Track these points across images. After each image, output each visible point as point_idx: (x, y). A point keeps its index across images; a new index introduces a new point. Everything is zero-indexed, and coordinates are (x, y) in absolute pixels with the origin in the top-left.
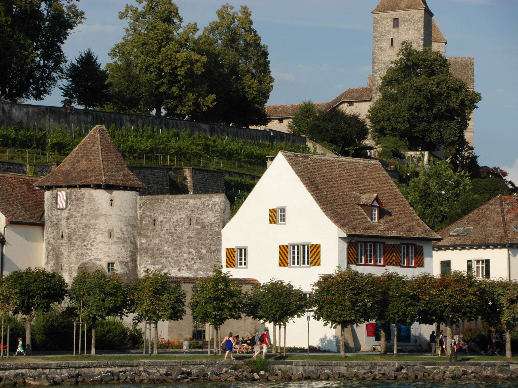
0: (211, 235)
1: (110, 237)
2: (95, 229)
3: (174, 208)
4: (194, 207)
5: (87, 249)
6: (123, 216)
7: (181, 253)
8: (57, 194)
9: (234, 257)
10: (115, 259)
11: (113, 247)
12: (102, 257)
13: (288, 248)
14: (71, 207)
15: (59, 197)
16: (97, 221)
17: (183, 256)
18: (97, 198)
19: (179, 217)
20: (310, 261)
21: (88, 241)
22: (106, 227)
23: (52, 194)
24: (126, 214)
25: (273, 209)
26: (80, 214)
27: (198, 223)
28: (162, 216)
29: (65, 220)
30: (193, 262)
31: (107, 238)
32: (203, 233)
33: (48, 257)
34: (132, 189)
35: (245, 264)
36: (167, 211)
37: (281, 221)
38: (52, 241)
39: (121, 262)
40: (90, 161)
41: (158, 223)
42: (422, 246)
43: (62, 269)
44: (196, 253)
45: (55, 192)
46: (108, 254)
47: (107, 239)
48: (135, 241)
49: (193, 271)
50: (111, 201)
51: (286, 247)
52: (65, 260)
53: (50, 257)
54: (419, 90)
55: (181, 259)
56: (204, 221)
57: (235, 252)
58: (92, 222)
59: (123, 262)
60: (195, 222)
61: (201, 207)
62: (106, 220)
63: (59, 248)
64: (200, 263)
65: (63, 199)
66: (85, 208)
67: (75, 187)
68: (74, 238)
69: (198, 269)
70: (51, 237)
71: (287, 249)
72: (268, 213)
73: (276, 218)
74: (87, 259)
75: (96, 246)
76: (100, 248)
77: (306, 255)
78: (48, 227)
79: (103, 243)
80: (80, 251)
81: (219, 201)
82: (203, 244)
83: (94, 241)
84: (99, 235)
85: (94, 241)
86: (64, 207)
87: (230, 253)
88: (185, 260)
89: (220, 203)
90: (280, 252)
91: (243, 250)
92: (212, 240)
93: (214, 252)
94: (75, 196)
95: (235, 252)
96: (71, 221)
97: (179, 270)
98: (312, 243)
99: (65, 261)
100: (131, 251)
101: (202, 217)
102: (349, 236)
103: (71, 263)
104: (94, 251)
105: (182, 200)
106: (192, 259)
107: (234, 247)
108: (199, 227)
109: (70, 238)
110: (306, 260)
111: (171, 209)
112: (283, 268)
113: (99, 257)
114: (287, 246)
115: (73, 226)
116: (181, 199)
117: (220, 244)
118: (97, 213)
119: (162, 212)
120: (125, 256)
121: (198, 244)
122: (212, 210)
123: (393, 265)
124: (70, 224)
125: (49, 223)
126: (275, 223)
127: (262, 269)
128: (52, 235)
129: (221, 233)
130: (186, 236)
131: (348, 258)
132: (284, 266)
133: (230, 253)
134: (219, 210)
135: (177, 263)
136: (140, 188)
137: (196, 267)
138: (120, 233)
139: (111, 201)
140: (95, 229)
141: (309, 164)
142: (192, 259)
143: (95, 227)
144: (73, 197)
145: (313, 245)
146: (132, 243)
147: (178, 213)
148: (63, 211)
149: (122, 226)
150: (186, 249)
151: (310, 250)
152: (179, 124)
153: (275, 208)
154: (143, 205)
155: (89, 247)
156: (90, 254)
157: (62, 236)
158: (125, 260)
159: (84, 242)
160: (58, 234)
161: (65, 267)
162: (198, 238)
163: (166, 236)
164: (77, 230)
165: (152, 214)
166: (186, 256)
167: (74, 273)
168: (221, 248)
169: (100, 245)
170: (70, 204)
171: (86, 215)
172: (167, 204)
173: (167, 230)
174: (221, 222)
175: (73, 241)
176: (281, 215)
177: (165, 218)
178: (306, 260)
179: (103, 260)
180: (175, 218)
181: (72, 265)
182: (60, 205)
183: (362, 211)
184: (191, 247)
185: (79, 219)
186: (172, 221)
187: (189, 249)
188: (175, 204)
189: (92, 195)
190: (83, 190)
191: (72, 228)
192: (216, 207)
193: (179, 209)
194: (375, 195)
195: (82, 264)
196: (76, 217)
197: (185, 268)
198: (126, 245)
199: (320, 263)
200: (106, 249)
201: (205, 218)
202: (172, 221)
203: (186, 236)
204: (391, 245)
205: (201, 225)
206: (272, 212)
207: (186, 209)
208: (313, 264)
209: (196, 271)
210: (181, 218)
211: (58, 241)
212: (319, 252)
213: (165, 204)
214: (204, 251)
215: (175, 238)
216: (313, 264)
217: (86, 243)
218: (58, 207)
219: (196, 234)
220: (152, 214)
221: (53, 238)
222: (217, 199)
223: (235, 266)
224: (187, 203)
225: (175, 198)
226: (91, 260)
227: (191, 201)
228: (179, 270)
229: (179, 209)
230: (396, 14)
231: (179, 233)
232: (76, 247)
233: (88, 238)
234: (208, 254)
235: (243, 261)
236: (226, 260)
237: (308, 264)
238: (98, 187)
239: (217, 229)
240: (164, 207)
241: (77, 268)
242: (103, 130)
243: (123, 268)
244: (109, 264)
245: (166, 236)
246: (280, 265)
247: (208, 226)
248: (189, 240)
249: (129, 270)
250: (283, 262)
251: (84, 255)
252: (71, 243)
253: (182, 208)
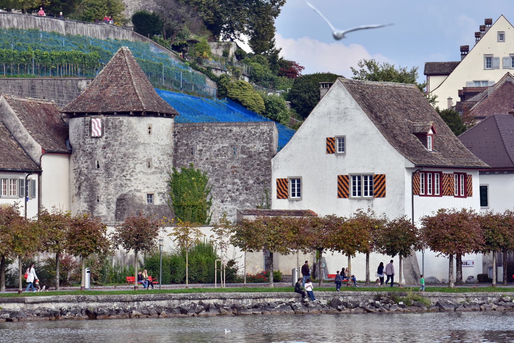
0: (258, 165)
1: (149, 167)
2: (134, 158)
3: (215, 136)
4: (238, 135)
5: (126, 180)
6: (160, 144)
7: (224, 183)
8: (91, 122)
9: (287, 188)
10: (153, 190)
11: (152, 177)
12: (142, 188)
13: (348, 179)
14: (108, 136)
15: (93, 125)
16: (136, 150)
17: (226, 187)
18: (135, 126)
19: (221, 145)
20: (374, 192)
21: (127, 171)
22: (144, 157)
23: (84, 122)
24: (163, 143)
25: (331, 138)
26: (118, 143)
27: (243, 152)
28: (201, 144)
29: (101, 149)
30: (238, 193)
31: (146, 167)
32: (250, 162)
33: (79, 188)
34: (168, 116)
35: (299, 195)
36: (206, 139)
37: (340, 150)
38: (86, 172)
39: (159, 193)
40: (122, 86)
41: (196, 152)
42: (471, 175)
43: (98, 201)
44: (241, 183)
45: (88, 119)
46: (147, 185)
47: (145, 169)
48: (170, 170)
49: (238, 202)
50: (149, 128)
51: (346, 178)
52: (101, 191)
53: (83, 188)
55: (224, 190)
56: (251, 150)
57: (287, 182)
58: (131, 151)
59: (161, 193)
60: (240, 151)
61: (246, 135)
62: (144, 149)
63: (95, 179)
64: (246, 194)
65: (98, 126)
66: (123, 137)
67: (111, 114)
68: (112, 168)
69: (244, 200)
70: (83, 167)
71: (347, 180)
72: (324, 143)
73: (334, 147)
74: (126, 191)
75: (136, 177)
76: (139, 178)
77: (369, 186)
78: (79, 156)
79: (142, 173)
80: (119, 182)
81: (268, 130)
82: (250, 175)
83: (133, 171)
84: (138, 165)
85: (133, 171)
86: (100, 134)
87: (282, 184)
88: (229, 191)
89: (269, 131)
90: (339, 183)
91: (297, 182)
92: (260, 170)
93: (262, 182)
94: (112, 123)
95: (287, 182)
96: (107, 150)
97: (222, 202)
98: (376, 174)
99: (101, 192)
100: (167, 182)
101: (248, 146)
102: (416, 166)
103: (109, 195)
104: (134, 181)
105: (225, 128)
106: (237, 190)
107: (286, 178)
108: (245, 156)
109: (107, 168)
110: (369, 191)
111: (211, 137)
112: (343, 200)
113: (139, 188)
114: (347, 176)
115: (111, 155)
116: (223, 126)
117: (270, 175)
118: (136, 142)
119: (201, 140)
120: (163, 186)
121: (244, 174)
122: (259, 138)
123: (449, 195)
124: (107, 153)
125: (81, 152)
126: (333, 152)
127: (322, 202)
128: (85, 165)
129: (270, 163)
130: (229, 166)
131: (413, 188)
132: (345, 197)
133: (282, 184)
134: (268, 139)
136: (174, 115)
137: (241, 198)
138: (158, 162)
139: (149, 128)
140: (134, 158)
141: (364, 91)
142: (237, 190)
143: (133, 156)
144: (110, 125)
145: (377, 175)
146: (168, 173)
147: (219, 141)
148: (98, 140)
149: (159, 155)
150: (230, 179)
151: (374, 181)
152: (43, 21)
153: (333, 136)
154: (178, 132)
155: (128, 177)
156: (129, 185)
157: (98, 166)
158: (163, 191)
159: (123, 172)
160: (92, 163)
161: (102, 198)
162: (244, 168)
163: (206, 166)
164: (115, 159)
165: (189, 142)
166: (230, 187)
167: (112, 205)
168: (270, 179)
169: (139, 175)
170: (106, 132)
171: (125, 144)
172: (206, 132)
173: (207, 159)
174: (271, 151)
175: (111, 171)
176: (340, 145)
177: (205, 146)
178: (369, 191)
179: (143, 191)
180: (216, 147)
181: (110, 197)
182: (94, 133)
183: (418, 139)
184: (235, 177)
185: (117, 147)
186: (213, 149)
187: (233, 179)
188: (216, 132)
189: (129, 123)
190: (121, 118)
191: (109, 157)
192: (265, 135)
193: (221, 138)
194: (431, 124)
195: (121, 195)
196: (113, 146)
197: (229, 199)
198: (163, 175)
199: (385, 194)
200: (145, 180)
201: (252, 148)
202: (213, 149)
203: (229, 166)
204: (447, 174)
205: (247, 154)
206: (330, 142)
207: (229, 137)
208: (377, 195)
209: (242, 203)
210: (223, 147)
211: (92, 171)
212: (385, 182)
213: (204, 132)
214: (251, 182)
215: (216, 167)
216: (377, 195)
217: (125, 173)
218: (93, 135)
219: (241, 164)
220: (189, 142)
221: (87, 168)
222: (266, 127)
223: (287, 197)
224: (231, 131)
225: (216, 126)
226: (130, 191)
227: (235, 129)
228: (222, 202)
229: (221, 138)
231: (222, 163)
232: (115, 177)
233: (127, 168)
234: (256, 185)
235: (296, 192)
236: (277, 191)
237: (371, 194)
238: (138, 114)
239: (266, 159)
241: (115, 200)
242: (128, 52)
243: (161, 200)
244: (148, 195)
245: (206, 166)
246: (339, 196)
247: (255, 155)
248: (233, 169)
249: (166, 202)
250: (343, 193)
251: (123, 186)
252: (109, 172)
253: (223, 137)
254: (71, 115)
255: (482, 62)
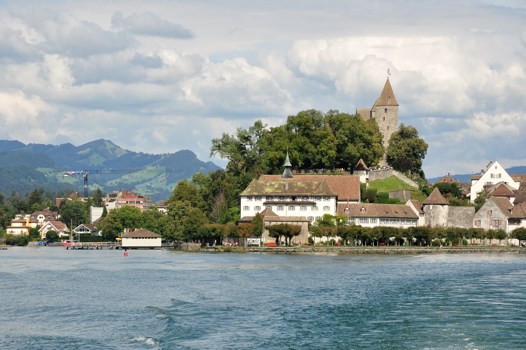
54: (409, 145)
109: (433, 217)
135: (460, 224)
230: (386, 107)
238: (441, 204)
240: (456, 209)
254: (424, 204)
255: (490, 176)
